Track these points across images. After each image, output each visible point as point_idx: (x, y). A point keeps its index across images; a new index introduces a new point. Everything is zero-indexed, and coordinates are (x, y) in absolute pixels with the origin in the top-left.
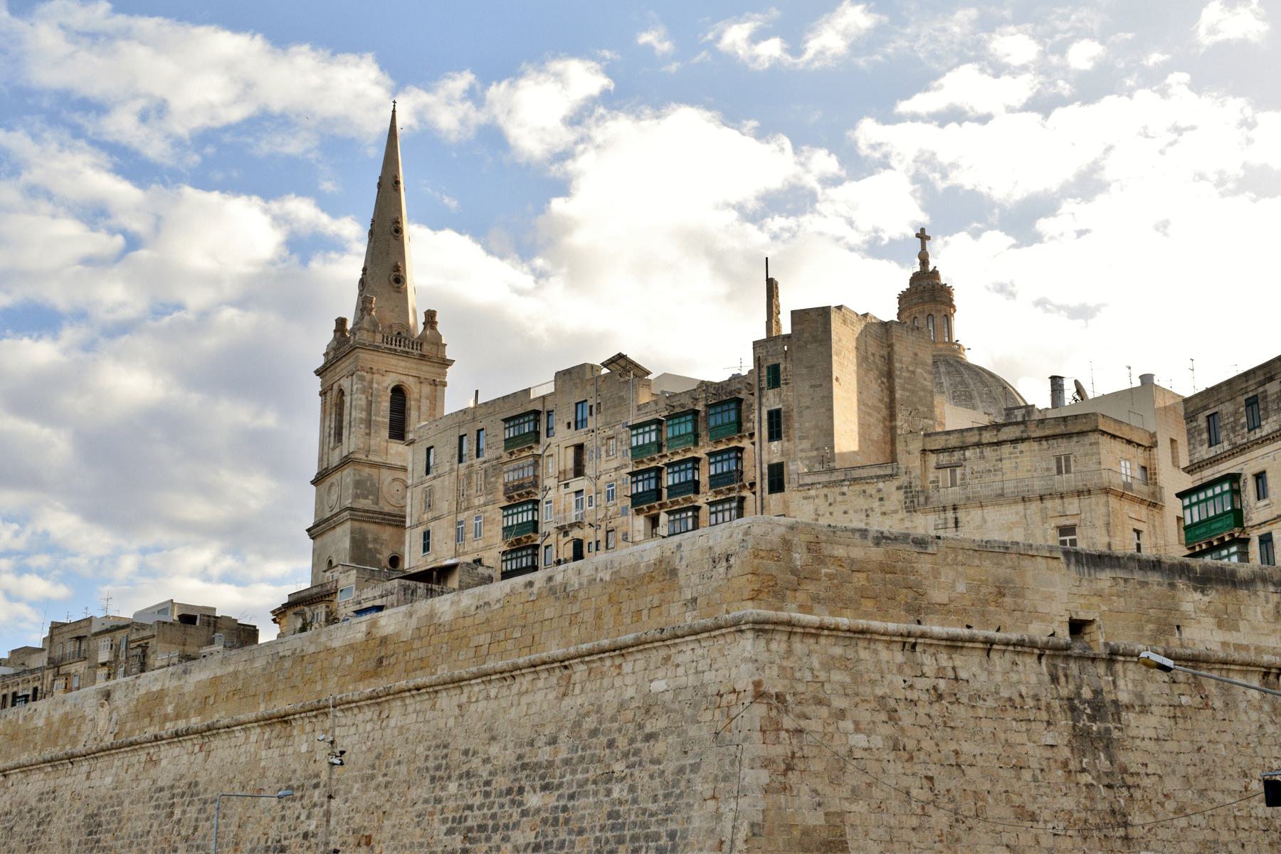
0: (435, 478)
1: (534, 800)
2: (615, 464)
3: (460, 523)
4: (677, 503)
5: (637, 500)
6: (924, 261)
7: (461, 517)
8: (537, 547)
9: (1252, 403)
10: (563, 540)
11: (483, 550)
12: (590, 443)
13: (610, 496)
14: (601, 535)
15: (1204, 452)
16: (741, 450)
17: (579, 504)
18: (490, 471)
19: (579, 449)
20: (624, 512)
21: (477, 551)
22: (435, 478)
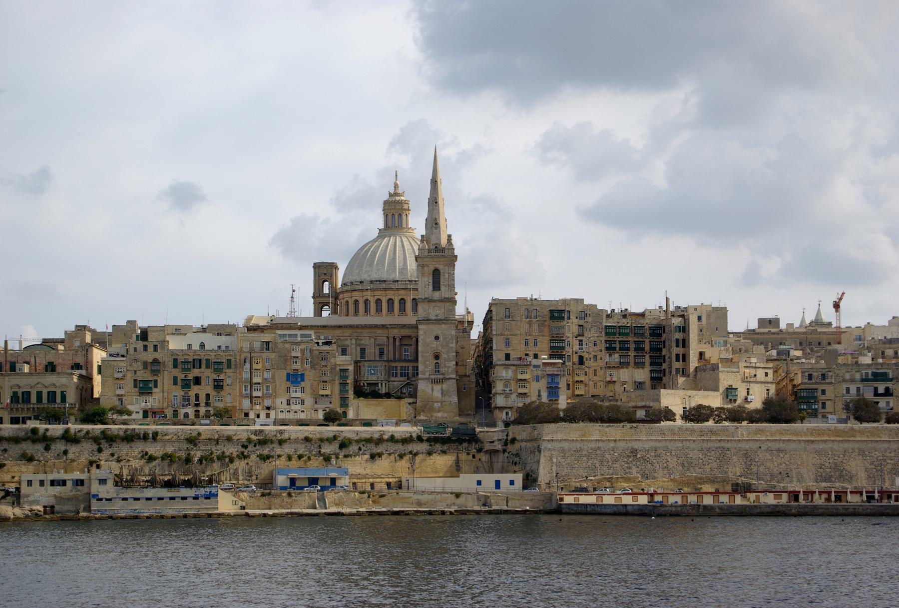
1: (889, 461)
2: (597, 335)
5: (607, 349)
6: (396, 186)
9: (823, 375)
10: (575, 355)
11: (538, 351)
12: (585, 325)
13: (595, 345)
14: (591, 356)
15: (806, 381)
16: (644, 341)
18: (540, 325)
20: (601, 351)
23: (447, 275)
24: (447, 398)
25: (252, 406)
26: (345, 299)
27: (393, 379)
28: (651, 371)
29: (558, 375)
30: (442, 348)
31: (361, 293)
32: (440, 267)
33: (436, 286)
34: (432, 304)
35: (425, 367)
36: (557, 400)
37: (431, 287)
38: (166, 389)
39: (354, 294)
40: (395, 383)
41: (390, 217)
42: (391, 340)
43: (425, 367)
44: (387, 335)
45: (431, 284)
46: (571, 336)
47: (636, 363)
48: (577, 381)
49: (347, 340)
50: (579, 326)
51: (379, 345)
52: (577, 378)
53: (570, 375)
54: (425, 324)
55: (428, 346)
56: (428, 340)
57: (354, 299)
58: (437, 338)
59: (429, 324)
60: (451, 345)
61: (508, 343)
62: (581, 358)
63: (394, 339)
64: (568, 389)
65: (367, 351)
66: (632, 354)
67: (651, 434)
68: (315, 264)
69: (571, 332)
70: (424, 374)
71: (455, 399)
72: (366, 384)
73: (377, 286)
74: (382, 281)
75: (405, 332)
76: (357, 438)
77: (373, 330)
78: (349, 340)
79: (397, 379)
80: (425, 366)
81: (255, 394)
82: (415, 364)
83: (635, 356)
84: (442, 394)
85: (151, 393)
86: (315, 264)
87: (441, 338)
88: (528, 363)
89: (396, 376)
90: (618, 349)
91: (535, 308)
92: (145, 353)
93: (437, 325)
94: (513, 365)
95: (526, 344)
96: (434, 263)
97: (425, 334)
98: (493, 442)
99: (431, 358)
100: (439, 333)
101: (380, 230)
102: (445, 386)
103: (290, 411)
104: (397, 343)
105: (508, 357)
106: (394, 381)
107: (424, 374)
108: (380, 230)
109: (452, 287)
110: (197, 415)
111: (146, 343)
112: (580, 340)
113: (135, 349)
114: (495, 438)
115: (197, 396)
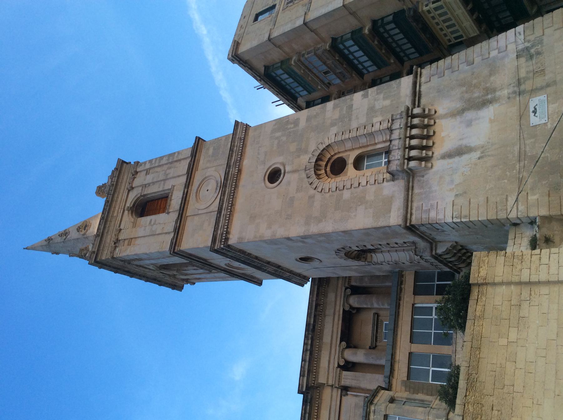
30: (306, 152)
34: (190, 211)
42: (348, 378)
55: (292, 199)
63: (349, 366)
84: (484, 104)
87: (276, 162)
93: (242, 183)
100: (262, 171)
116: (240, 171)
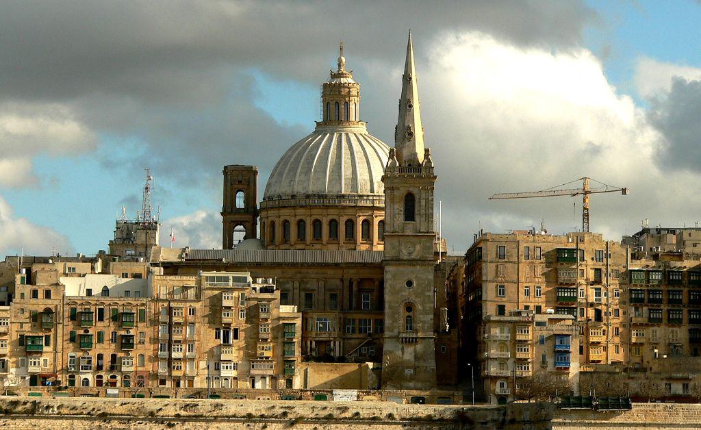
0: (506, 262)
3: (526, 287)
4: (653, 306)
7: (527, 285)
8: (576, 308)
16: (682, 291)
17: (598, 293)
19: (598, 271)
21: (538, 303)
22: (506, 262)
23: (423, 202)
24: (421, 363)
25: (170, 372)
26: (270, 219)
27: (349, 336)
28: (690, 331)
29: (569, 335)
30: (416, 297)
31: (293, 211)
32: (415, 191)
33: (410, 215)
35: (394, 322)
36: (568, 369)
37: (402, 218)
38: (59, 347)
39: (283, 211)
40: (353, 342)
41: (332, 106)
42: (347, 283)
43: (394, 322)
44: (340, 276)
45: (402, 213)
46: (583, 282)
47: (669, 320)
48: (593, 343)
49: (288, 283)
50: (596, 269)
51: (330, 290)
52: (593, 339)
53: (583, 334)
54: (396, 265)
56: (398, 287)
57: (282, 219)
58: (410, 283)
59: (400, 264)
60: (428, 294)
61: (501, 291)
62: (598, 312)
64: (581, 353)
65: (315, 297)
66: (664, 307)
67: (690, 417)
68: (226, 167)
69: (585, 278)
70: (392, 331)
71: (432, 364)
72: (314, 343)
73: (317, 202)
74: (322, 195)
75: (365, 274)
76: (313, 416)
77: (324, 270)
78: (291, 284)
79: (355, 336)
80: (393, 321)
81: (174, 355)
82: (379, 317)
83: (669, 311)
85: (41, 353)
86: (226, 167)
88: (530, 320)
89: (354, 331)
90: (646, 301)
91: (538, 245)
92: (33, 301)
93: (409, 267)
94: (510, 322)
95: (527, 293)
96: (406, 185)
97: (393, 279)
98: (486, 423)
99: (402, 309)
101: (318, 124)
102: (419, 347)
103: (218, 378)
104: (355, 288)
105: (501, 310)
106: (351, 339)
107: (392, 331)
108: (318, 124)
109: (429, 217)
110: (99, 383)
111: (34, 287)
112: (596, 289)
113: (22, 296)
114: (489, 419)
115: (100, 357)
116: (414, 265)
